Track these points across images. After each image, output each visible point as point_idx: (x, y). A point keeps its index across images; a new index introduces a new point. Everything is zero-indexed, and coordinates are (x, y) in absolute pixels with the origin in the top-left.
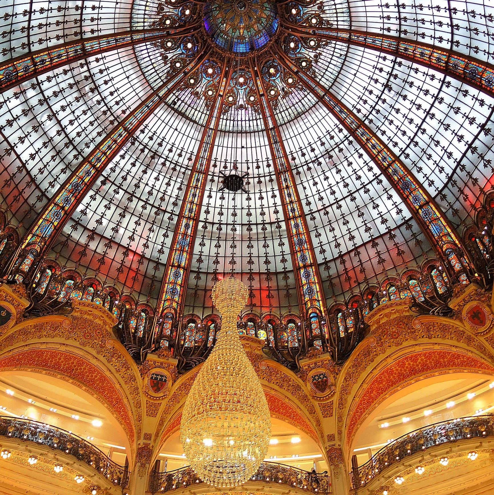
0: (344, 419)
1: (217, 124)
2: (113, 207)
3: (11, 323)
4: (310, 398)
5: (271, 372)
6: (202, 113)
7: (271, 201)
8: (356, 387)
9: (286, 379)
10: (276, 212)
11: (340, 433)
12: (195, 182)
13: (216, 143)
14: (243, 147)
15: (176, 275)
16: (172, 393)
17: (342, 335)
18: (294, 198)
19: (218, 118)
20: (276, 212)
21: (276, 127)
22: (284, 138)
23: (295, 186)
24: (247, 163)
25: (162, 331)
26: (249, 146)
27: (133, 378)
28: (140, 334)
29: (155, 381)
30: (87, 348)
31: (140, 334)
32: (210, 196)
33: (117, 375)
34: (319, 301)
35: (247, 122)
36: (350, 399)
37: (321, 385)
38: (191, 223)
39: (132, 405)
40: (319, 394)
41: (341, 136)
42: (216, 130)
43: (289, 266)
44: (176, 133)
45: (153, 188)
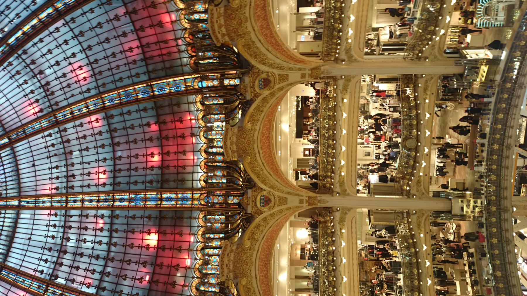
0: (291, 66)
1: (12, 198)
2: (124, 272)
4: (273, 90)
5: (253, 120)
6: (4, 218)
8: (270, 56)
9: (257, 109)
11: (300, 69)
14: (34, 165)
15: (169, 199)
16: (270, 189)
22: (19, 124)
23: (69, 105)
24: (50, 157)
26: (31, 159)
27: (265, 219)
29: (265, 203)
30: (254, 259)
33: (265, 231)
34: (185, 79)
35: (5, 167)
36: (278, 61)
37: (266, 83)
39: (281, 216)
40: (272, 84)
41: (15, 63)
42: (19, 197)
44: (33, 237)
45: (95, 242)
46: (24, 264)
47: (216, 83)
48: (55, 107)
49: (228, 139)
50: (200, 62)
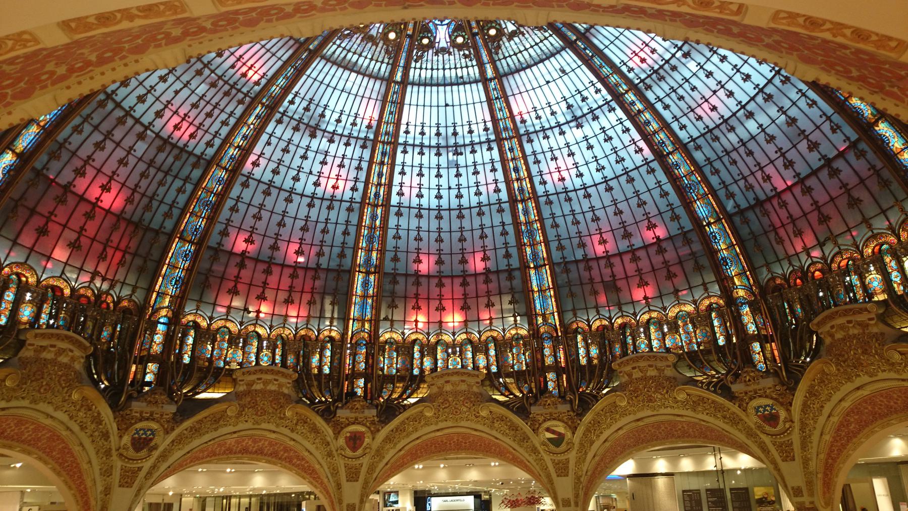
3: (157, 440)
7: (491, 177)
10: (497, 191)
12: (379, 157)
13: (407, 101)
14: (447, 105)
15: (365, 284)
17: (583, 361)
18: (523, 173)
19: (407, 68)
20: (497, 191)
21: (499, 76)
25: (354, 366)
26: (456, 102)
28: (326, 370)
31: (326, 370)
32: (403, 173)
38: (379, 211)
43: (515, 262)
46: (310, 81)
47: (549, 361)
48: (525, 139)
49: (463, 378)
50: (579, 338)
